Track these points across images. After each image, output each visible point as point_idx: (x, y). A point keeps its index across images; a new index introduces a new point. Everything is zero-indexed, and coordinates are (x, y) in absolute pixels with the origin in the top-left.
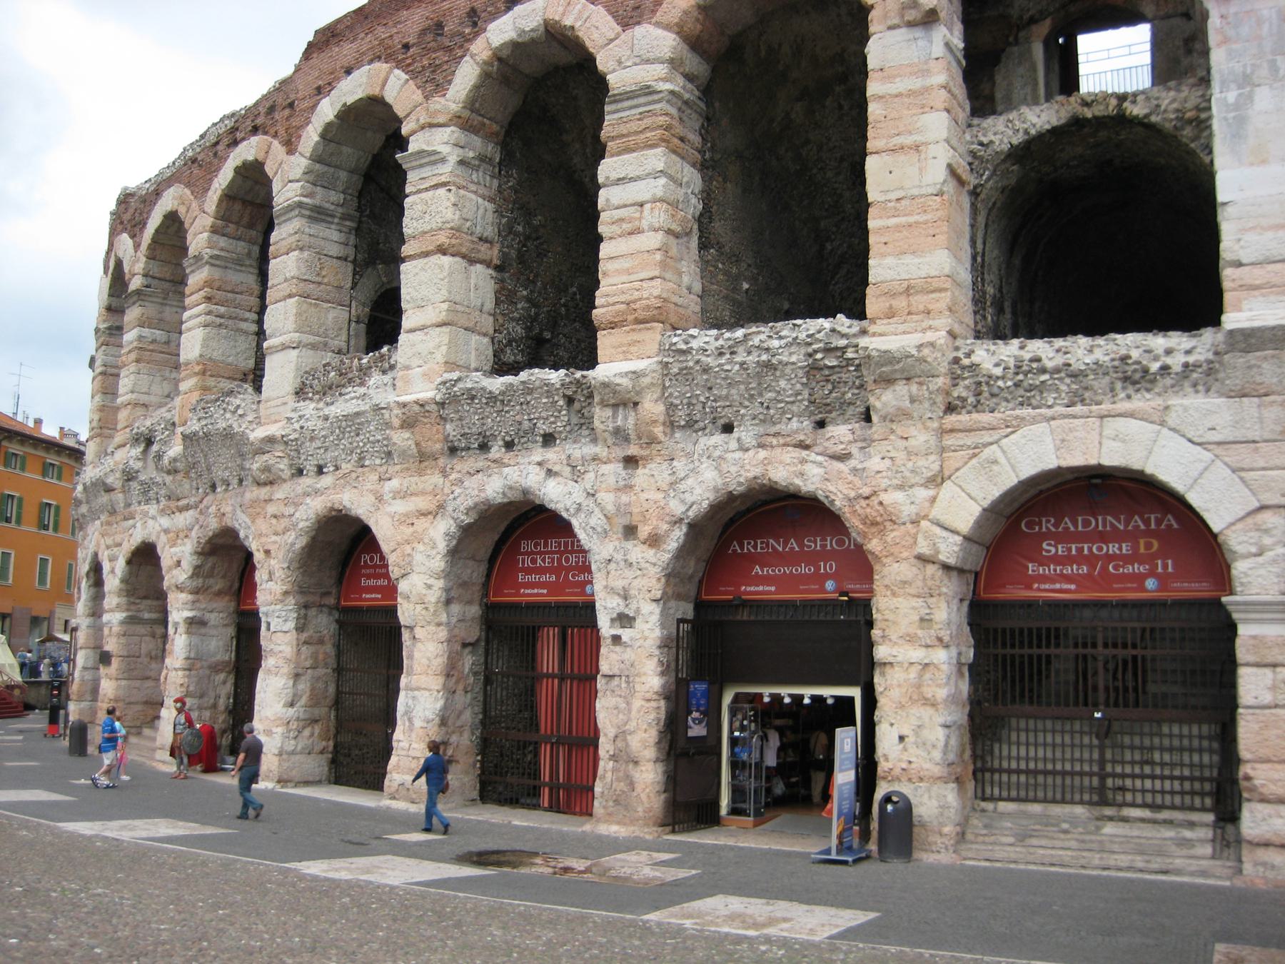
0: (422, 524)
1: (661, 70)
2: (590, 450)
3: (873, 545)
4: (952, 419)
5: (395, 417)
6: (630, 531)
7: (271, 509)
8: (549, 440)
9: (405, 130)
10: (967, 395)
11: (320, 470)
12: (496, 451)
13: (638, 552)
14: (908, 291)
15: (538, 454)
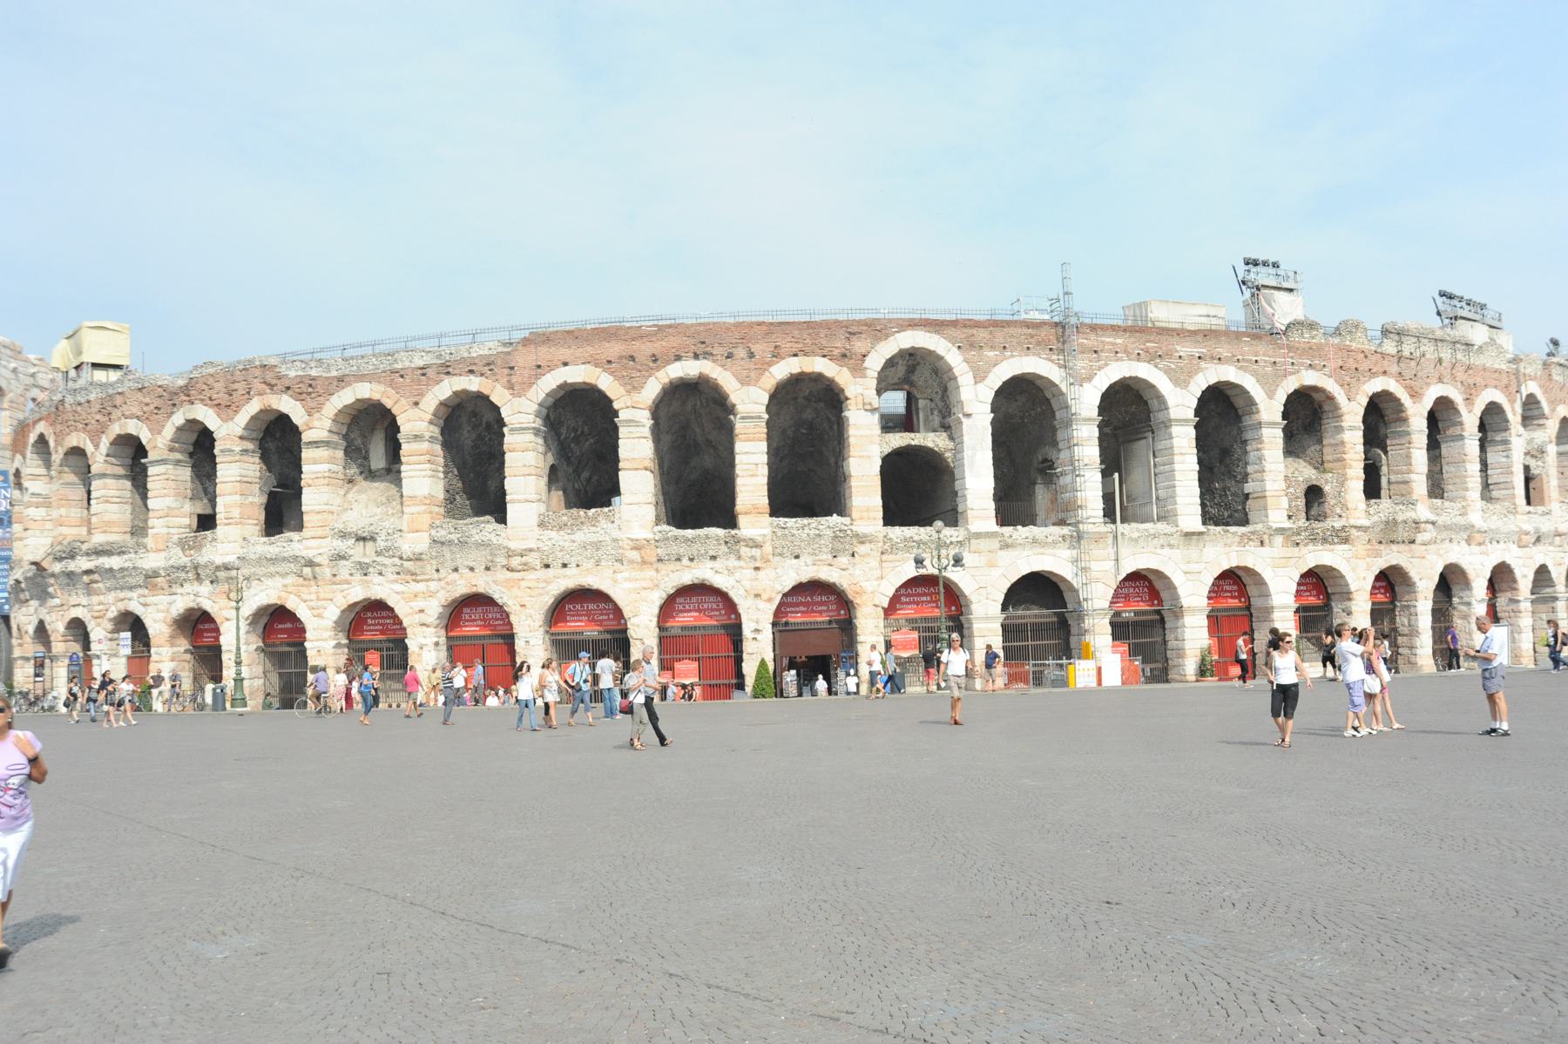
0: (644, 593)
1: (764, 408)
2: (737, 563)
3: (857, 601)
4: (885, 557)
5: (626, 544)
6: (757, 596)
7: (524, 584)
8: (714, 558)
9: (616, 406)
10: (890, 549)
11: (565, 565)
12: (685, 561)
13: (762, 605)
14: (868, 510)
15: (710, 564)
